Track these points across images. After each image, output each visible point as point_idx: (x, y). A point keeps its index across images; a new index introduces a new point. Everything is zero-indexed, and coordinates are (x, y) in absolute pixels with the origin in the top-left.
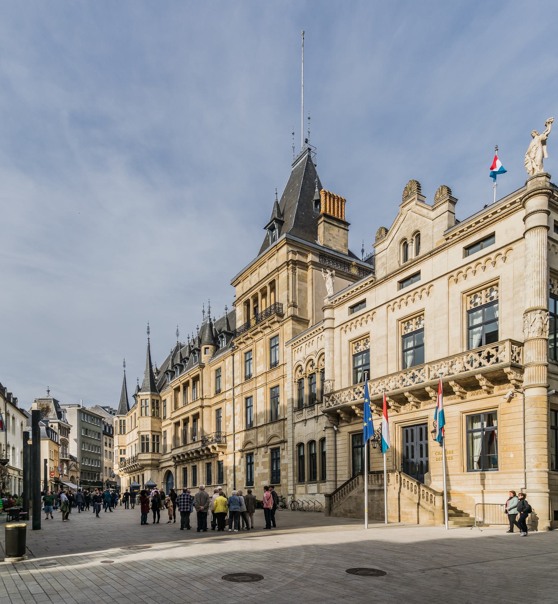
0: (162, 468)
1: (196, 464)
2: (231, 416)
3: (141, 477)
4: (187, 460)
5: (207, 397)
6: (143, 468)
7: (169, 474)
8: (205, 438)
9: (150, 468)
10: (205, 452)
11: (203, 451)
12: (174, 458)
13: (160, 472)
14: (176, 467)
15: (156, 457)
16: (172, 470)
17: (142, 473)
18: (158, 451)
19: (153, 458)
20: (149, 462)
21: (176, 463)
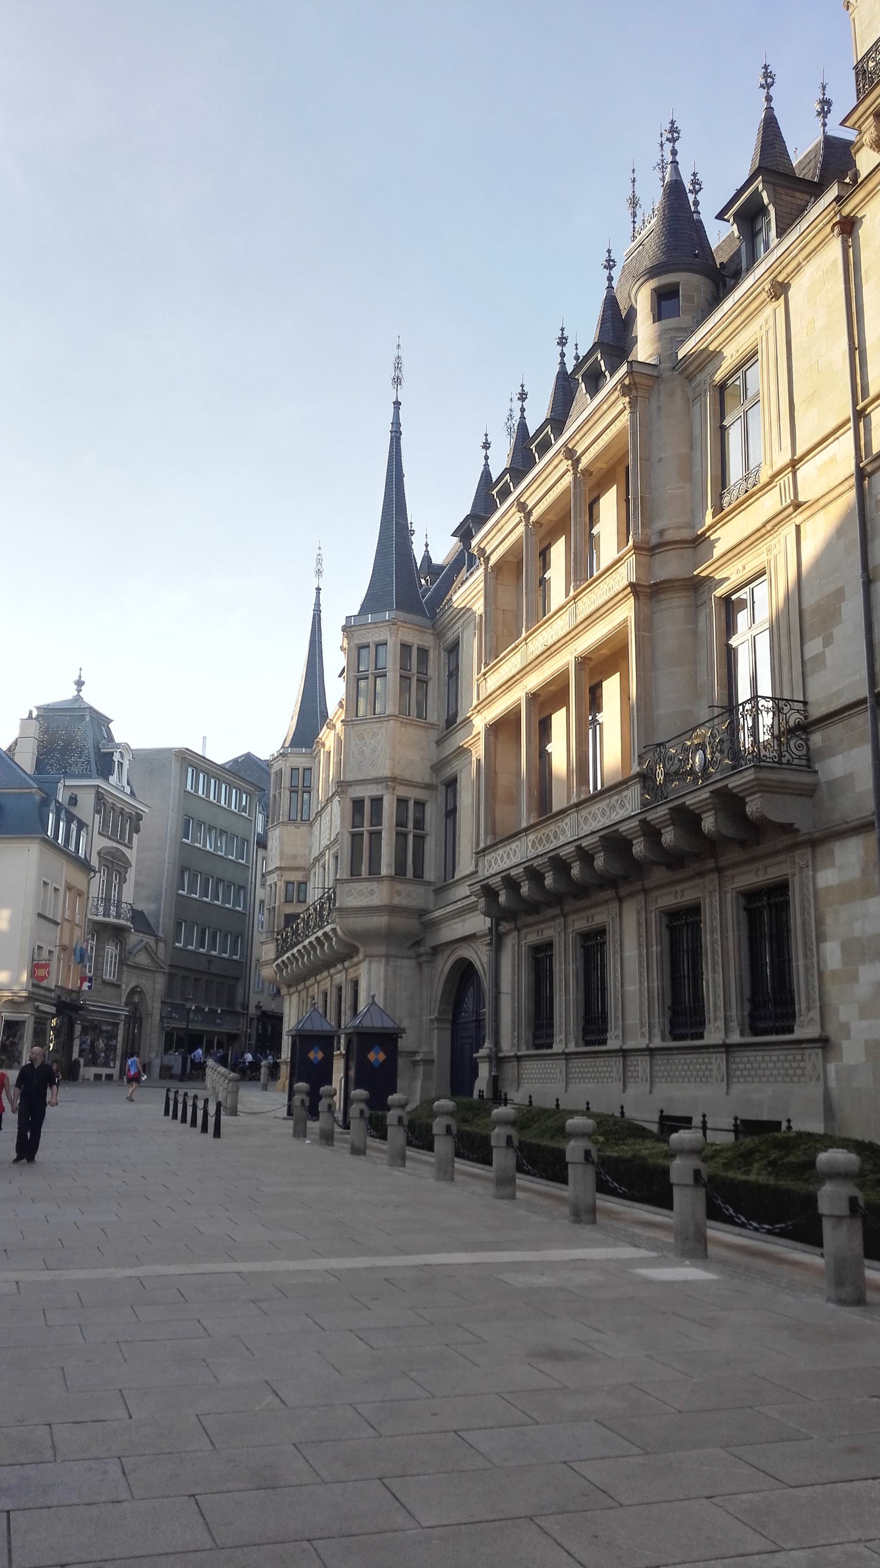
0: (436, 950)
1: (600, 917)
2: (839, 595)
3: (347, 994)
4: (555, 899)
5: (669, 536)
6: (355, 951)
7: (465, 973)
8: (665, 759)
9: (382, 950)
10: (668, 837)
11: (651, 832)
12: (489, 892)
13: (427, 970)
14: (497, 940)
15: (411, 895)
16: (479, 956)
17: (352, 974)
18: (419, 874)
19: (397, 901)
20: (380, 921)
21: (497, 922)
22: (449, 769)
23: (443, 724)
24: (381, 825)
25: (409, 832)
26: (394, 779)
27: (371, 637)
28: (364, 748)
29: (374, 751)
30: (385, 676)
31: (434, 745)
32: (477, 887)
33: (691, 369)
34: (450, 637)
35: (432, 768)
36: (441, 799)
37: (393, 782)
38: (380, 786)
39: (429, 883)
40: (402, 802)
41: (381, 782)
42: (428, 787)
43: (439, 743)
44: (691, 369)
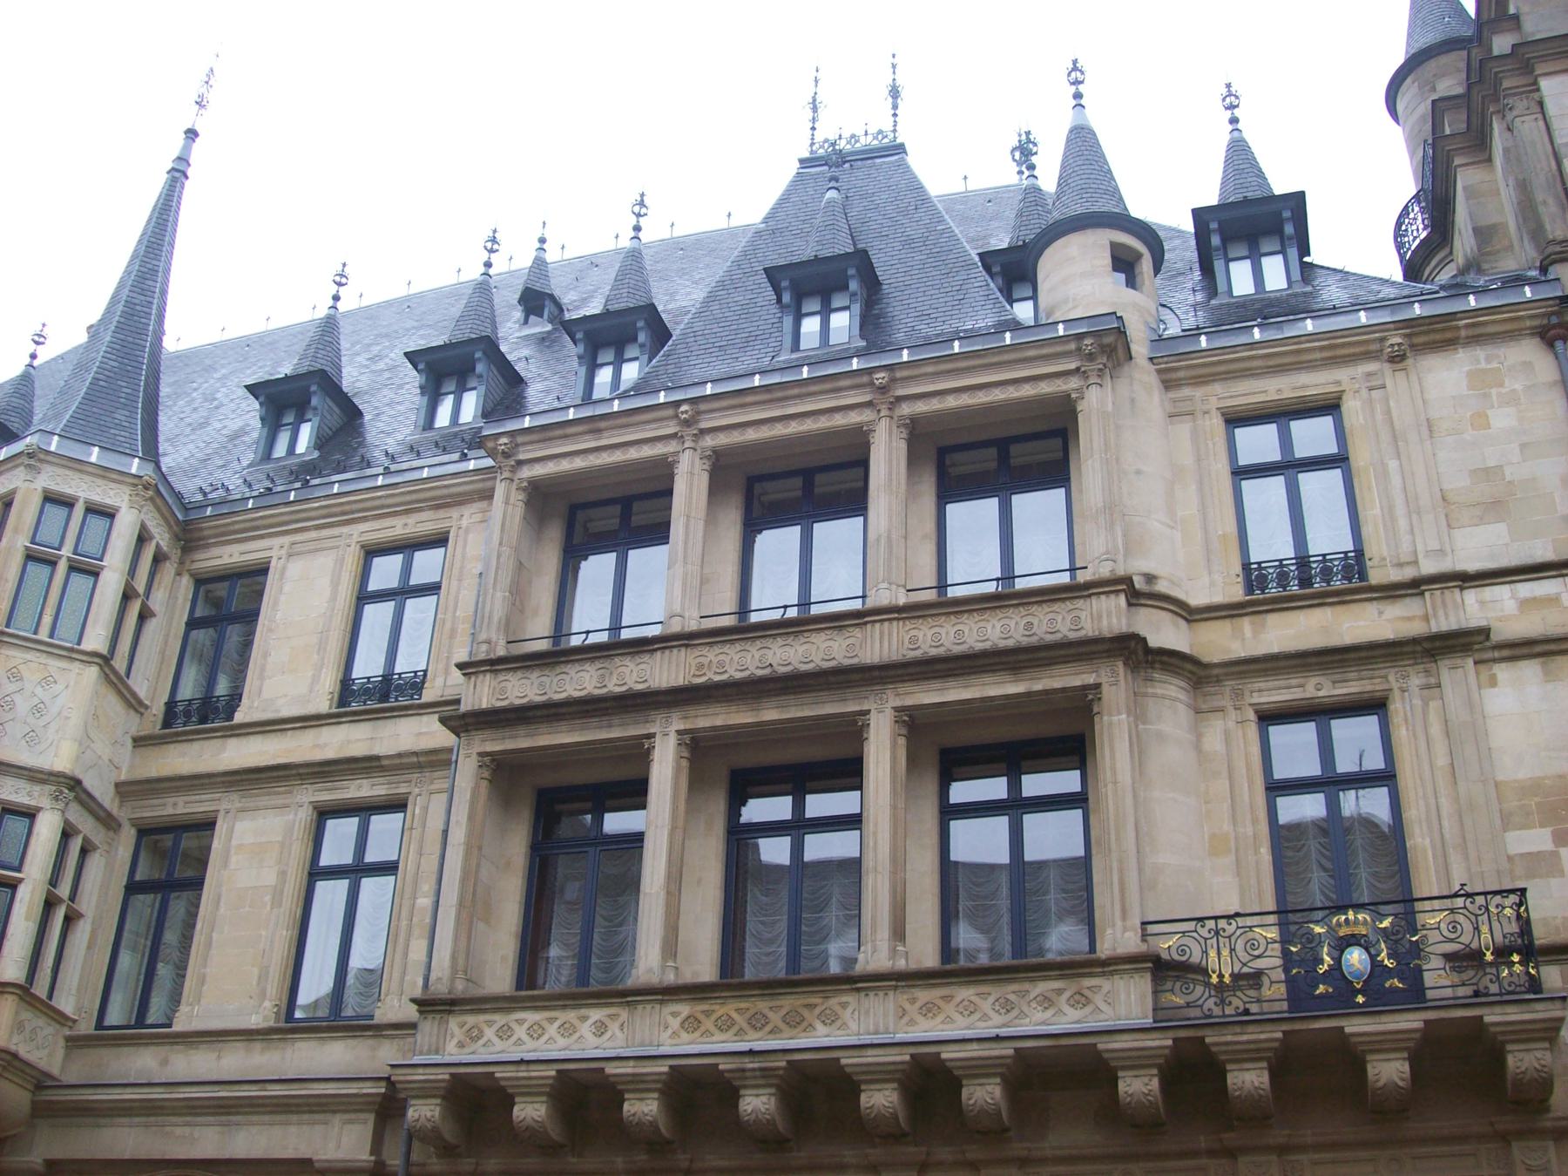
22: (181, 800)
23: (158, 708)
24: (19, 870)
25: (61, 901)
26: (75, 784)
27: (84, 489)
28: (18, 698)
29: (38, 710)
30: (96, 575)
31: (129, 743)
32: (443, 1075)
33: (1181, 374)
34: (230, 555)
35: (117, 785)
36: (124, 851)
37: (71, 789)
38: (37, 788)
39: (60, 1018)
40: (67, 834)
41: (43, 782)
42: (108, 821)
43: (140, 742)
44: (1181, 374)
